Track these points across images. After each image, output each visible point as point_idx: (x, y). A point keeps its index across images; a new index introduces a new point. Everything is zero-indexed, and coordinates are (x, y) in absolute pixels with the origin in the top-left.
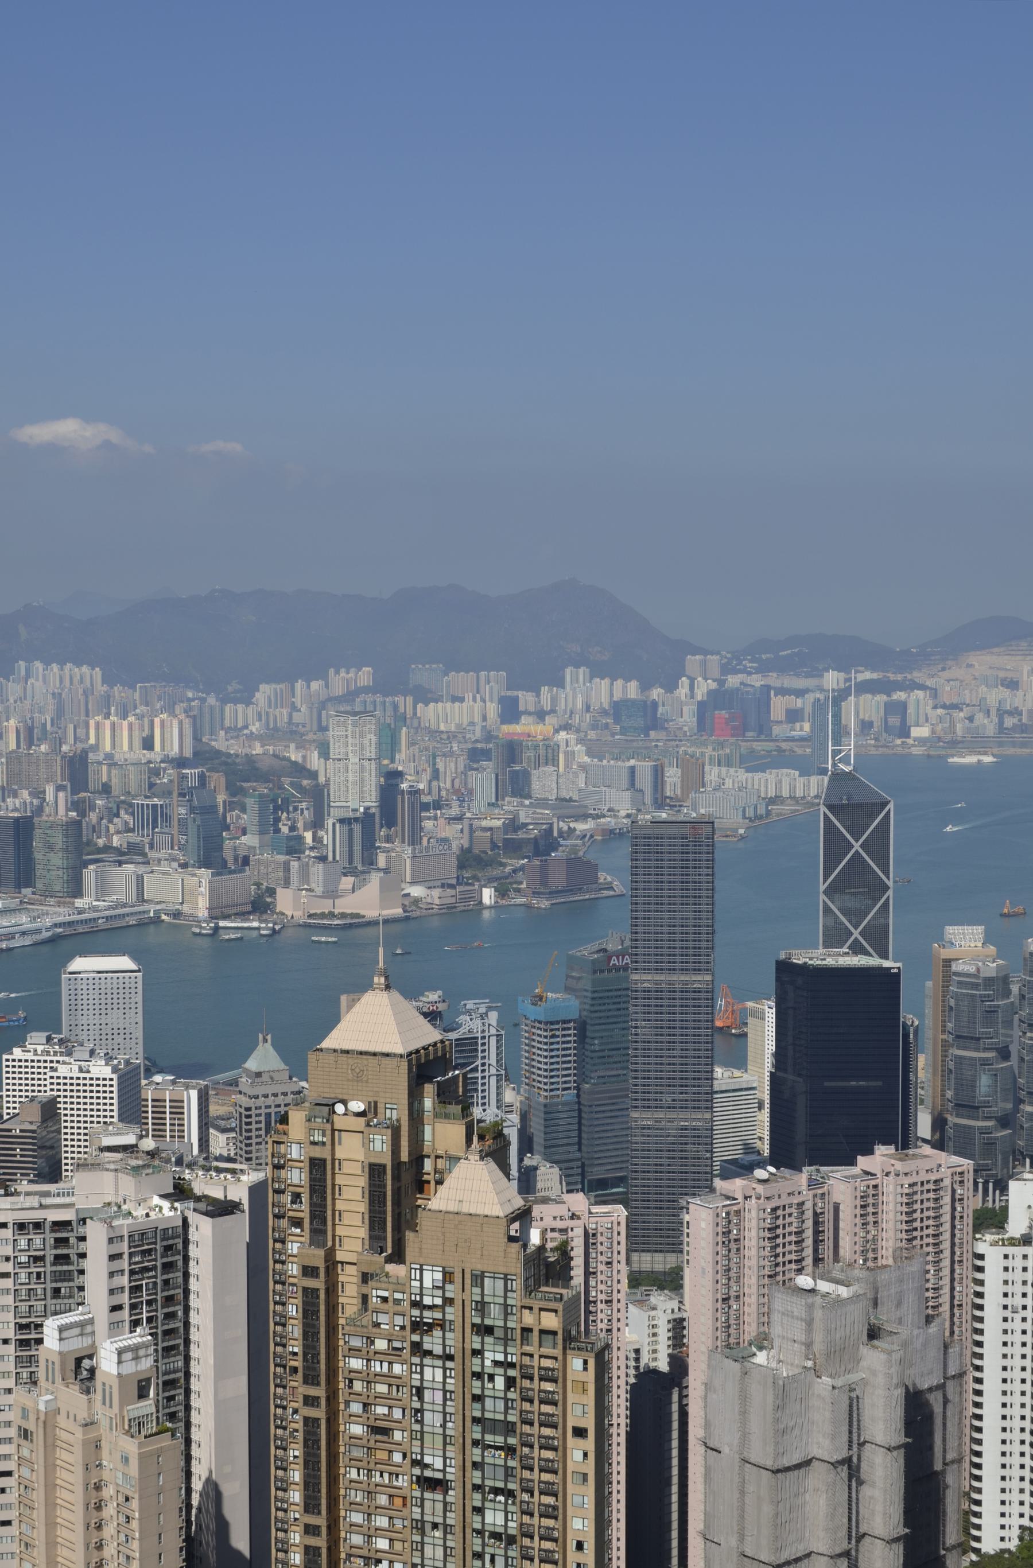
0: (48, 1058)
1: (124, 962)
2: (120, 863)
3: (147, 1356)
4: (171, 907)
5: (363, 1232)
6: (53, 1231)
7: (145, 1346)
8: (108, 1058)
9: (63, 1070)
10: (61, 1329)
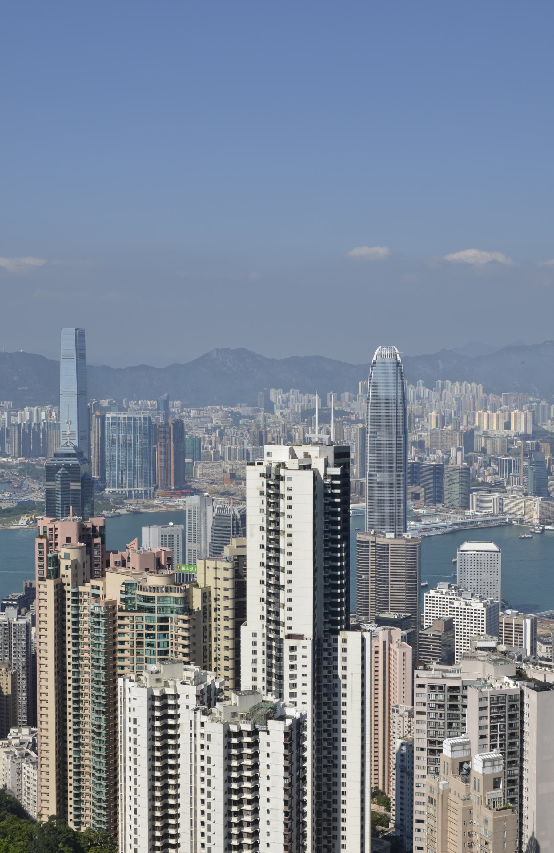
0: (449, 597)
1: (492, 546)
2: (490, 492)
3: (499, 765)
4: (518, 517)
6: (449, 691)
7: (499, 760)
8: (481, 599)
9: (456, 604)
10: (452, 746)
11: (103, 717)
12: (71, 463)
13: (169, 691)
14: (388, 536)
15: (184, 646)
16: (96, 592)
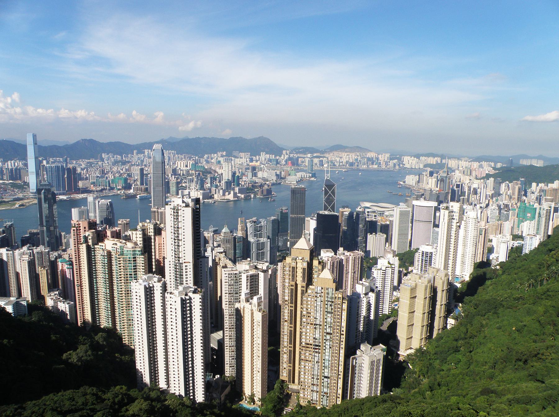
5: (301, 279)
11: (108, 290)
12: (47, 188)
13: (151, 285)
14: (162, 209)
15: (142, 266)
16: (101, 247)
